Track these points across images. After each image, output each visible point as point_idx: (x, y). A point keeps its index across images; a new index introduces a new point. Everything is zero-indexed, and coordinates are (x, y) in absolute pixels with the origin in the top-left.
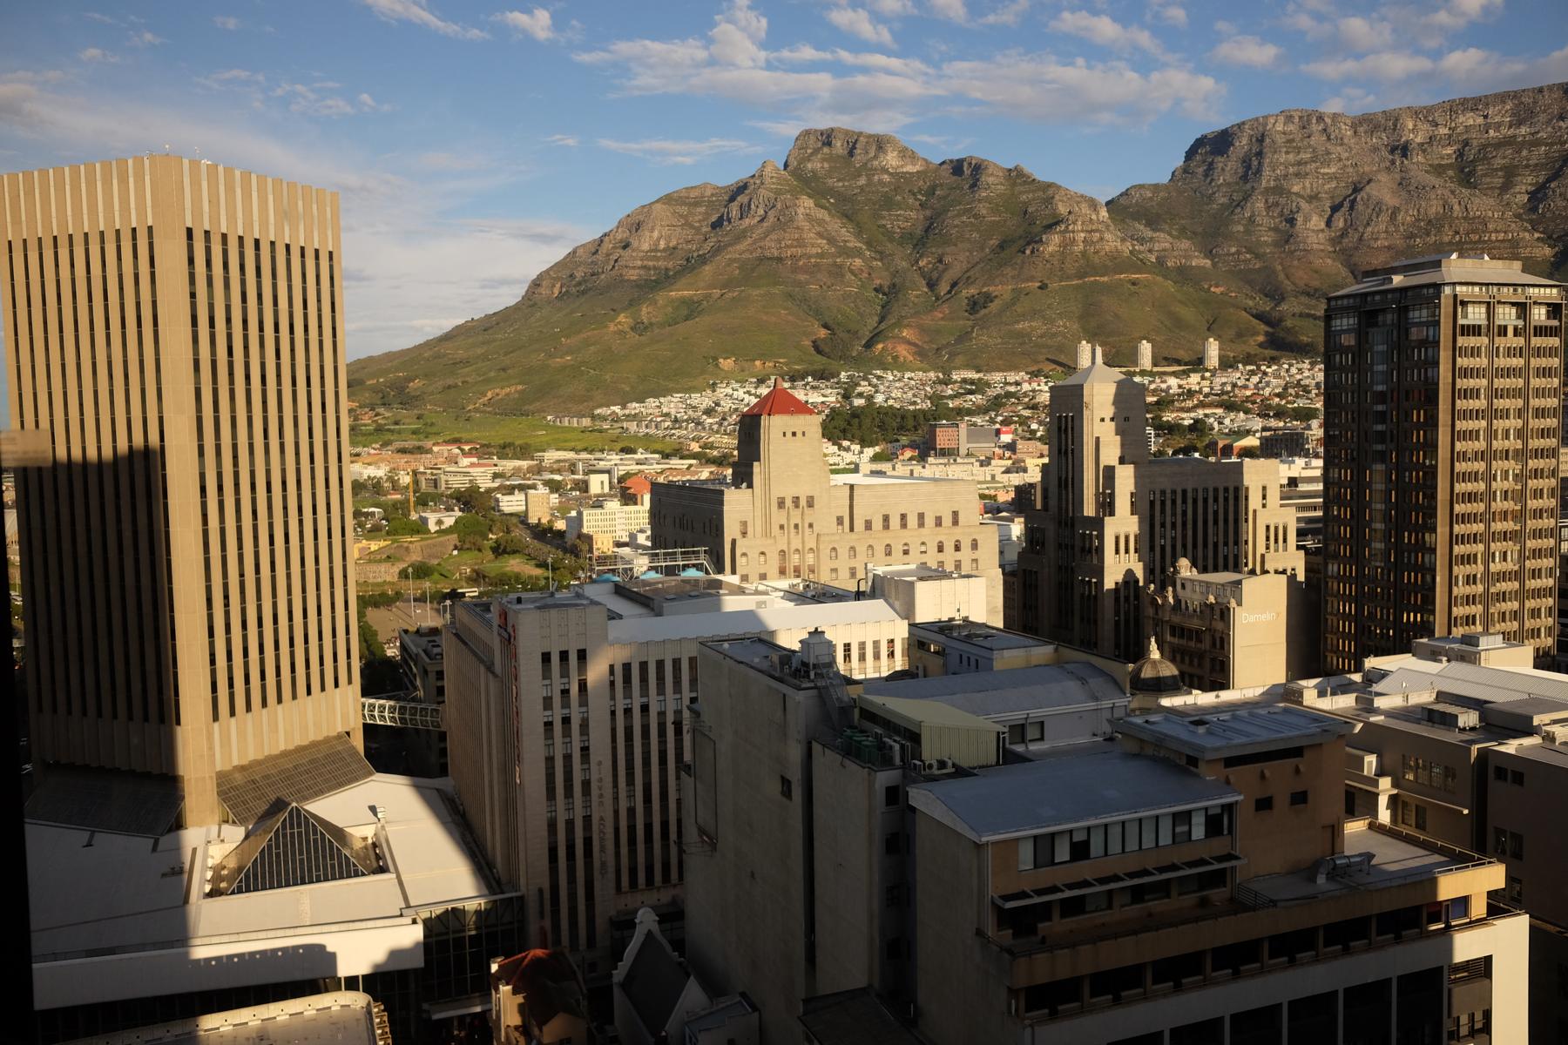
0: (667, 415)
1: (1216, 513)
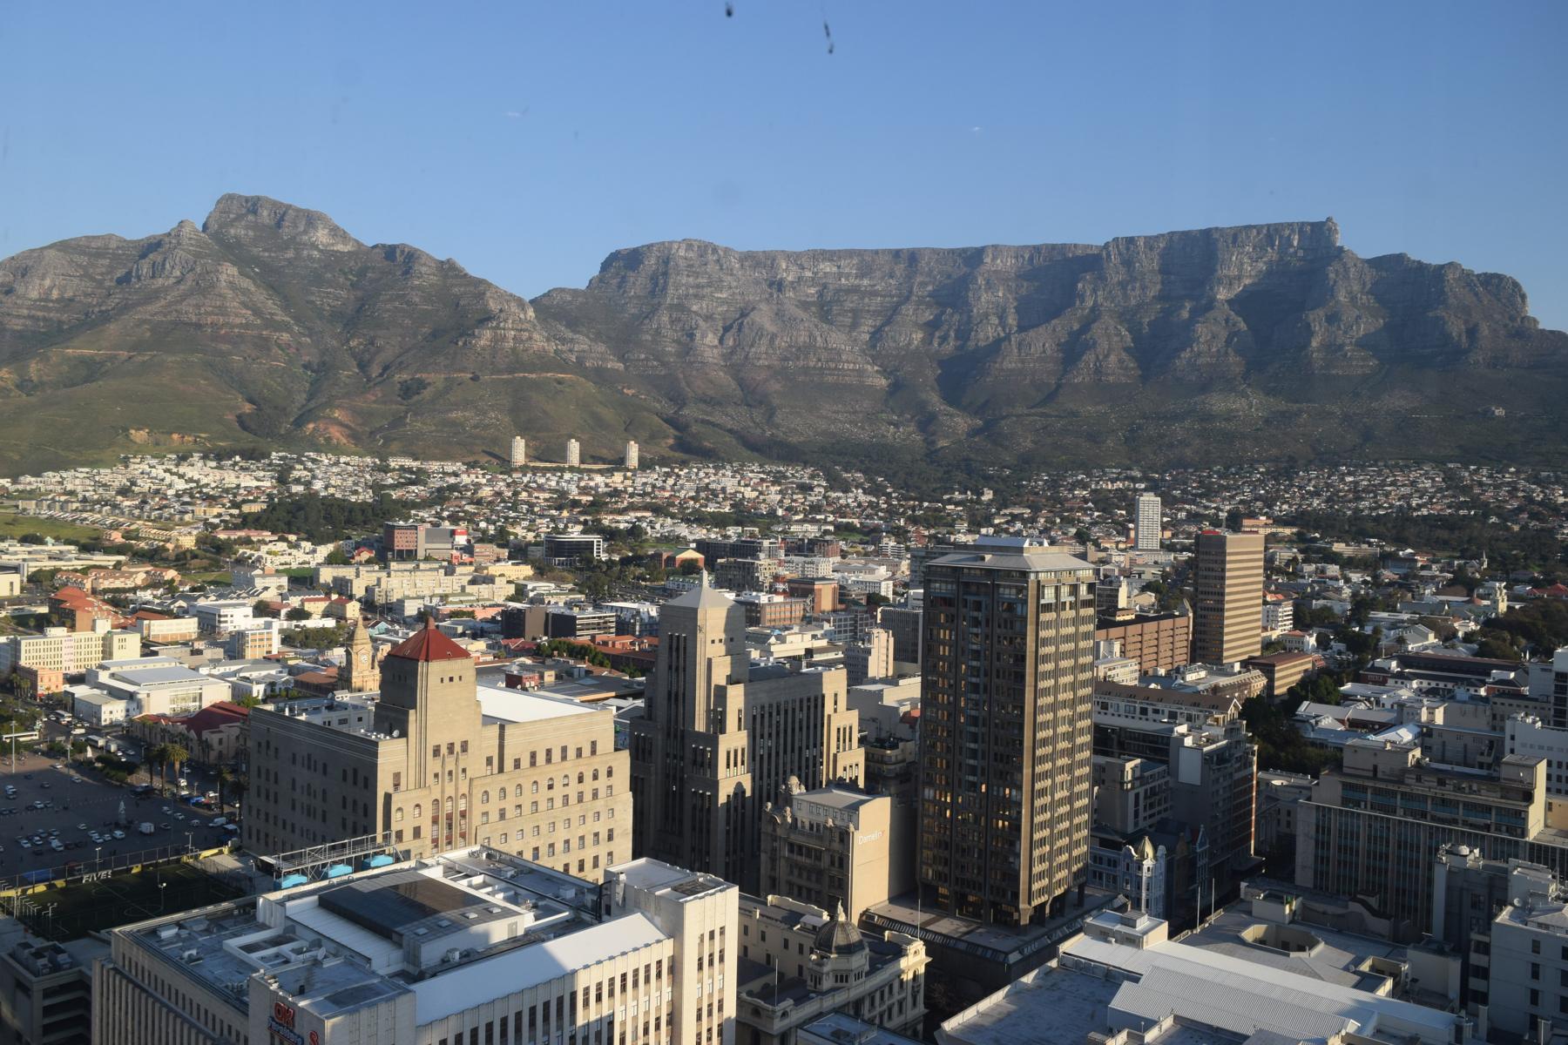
0: (72, 493)
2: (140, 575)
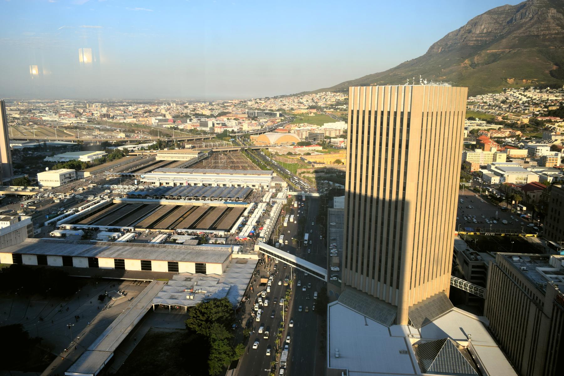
0: (485, 103)
2: (507, 132)
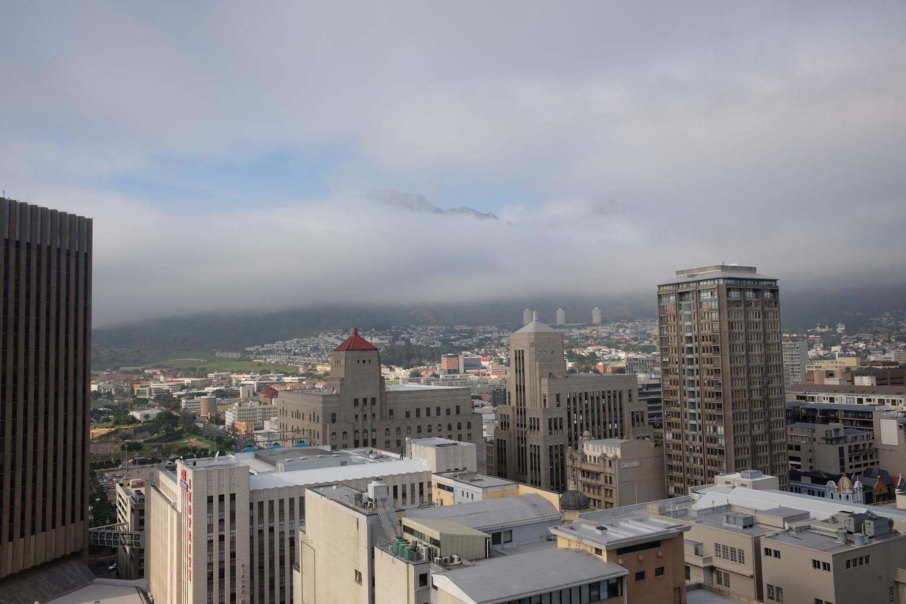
0: (290, 351)
1: (604, 406)
